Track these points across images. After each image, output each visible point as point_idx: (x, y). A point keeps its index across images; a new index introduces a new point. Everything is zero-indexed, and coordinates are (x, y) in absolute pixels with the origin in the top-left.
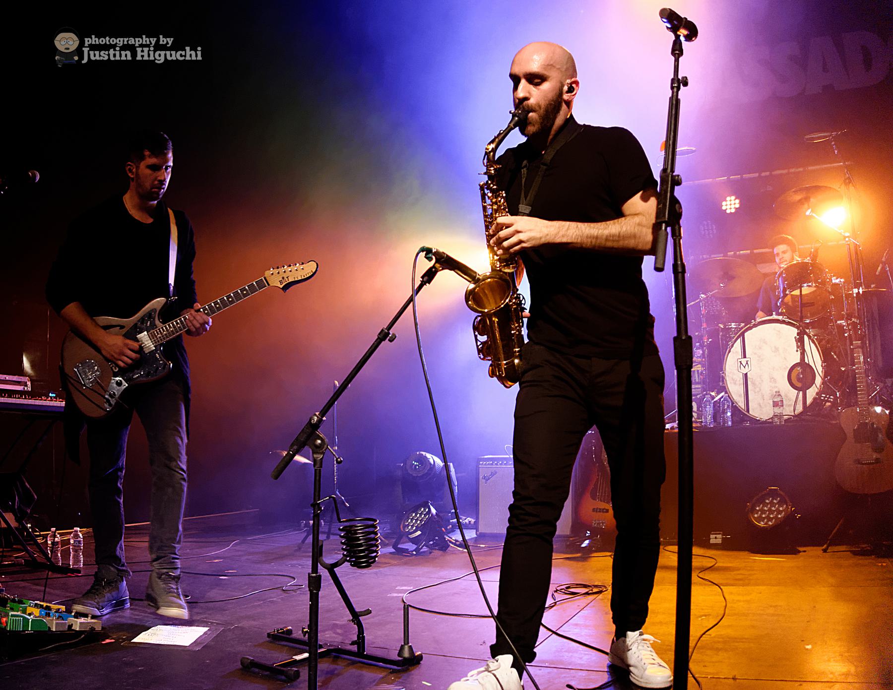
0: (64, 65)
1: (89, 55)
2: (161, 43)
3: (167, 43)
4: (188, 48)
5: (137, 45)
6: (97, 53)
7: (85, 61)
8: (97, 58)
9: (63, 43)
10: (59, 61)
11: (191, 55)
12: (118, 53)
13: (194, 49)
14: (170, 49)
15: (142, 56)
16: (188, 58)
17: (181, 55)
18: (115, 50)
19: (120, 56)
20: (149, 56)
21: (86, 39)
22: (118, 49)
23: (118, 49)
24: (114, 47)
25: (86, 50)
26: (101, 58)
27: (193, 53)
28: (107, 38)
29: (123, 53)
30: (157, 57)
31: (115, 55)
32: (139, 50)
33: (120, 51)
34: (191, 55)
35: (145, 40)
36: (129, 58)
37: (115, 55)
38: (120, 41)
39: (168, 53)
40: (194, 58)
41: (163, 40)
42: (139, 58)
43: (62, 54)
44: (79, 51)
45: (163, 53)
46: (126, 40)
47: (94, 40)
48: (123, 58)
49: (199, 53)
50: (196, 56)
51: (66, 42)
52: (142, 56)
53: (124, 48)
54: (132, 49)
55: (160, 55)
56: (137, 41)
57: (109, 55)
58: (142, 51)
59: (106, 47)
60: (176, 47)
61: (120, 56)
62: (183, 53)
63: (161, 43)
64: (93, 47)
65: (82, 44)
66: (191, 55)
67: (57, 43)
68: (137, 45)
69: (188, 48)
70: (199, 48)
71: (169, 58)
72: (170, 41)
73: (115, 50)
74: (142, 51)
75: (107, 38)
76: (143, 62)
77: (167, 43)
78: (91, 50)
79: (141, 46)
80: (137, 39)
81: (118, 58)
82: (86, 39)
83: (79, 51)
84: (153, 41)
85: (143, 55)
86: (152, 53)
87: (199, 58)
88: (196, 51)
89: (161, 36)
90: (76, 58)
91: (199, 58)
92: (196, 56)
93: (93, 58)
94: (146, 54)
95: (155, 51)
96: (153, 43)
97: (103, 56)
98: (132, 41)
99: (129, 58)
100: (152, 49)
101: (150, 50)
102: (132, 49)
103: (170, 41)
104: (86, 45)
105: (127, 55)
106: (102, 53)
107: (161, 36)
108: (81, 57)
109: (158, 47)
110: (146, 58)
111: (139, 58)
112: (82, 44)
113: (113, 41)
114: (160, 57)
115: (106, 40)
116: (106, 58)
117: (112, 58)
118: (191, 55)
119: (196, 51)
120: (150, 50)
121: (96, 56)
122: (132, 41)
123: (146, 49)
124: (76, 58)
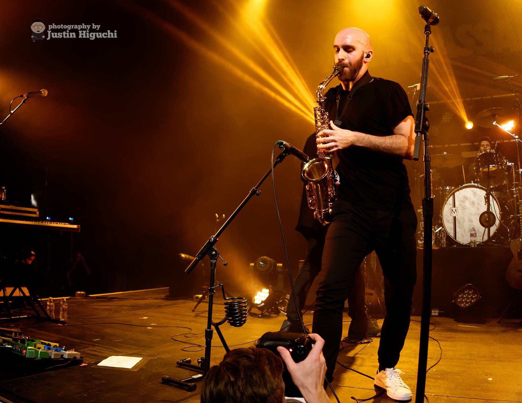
0: (36, 41)
1: (51, 35)
2: (93, 28)
3: (97, 28)
4: (109, 31)
5: (79, 29)
6: (56, 34)
7: (49, 38)
8: (56, 37)
9: (36, 28)
10: (34, 38)
11: (111, 35)
12: (68, 34)
13: (112, 31)
14: (98, 31)
15: (82, 36)
16: (109, 37)
17: (105, 35)
18: (66, 32)
19: (69, 35)
20: (86, 35)
21: (49, 26)
22: (68, 31)
23: (68, 31)
24: (66, 30)
25: (49, 32)
26: (58, 37)
27: (112, 34)
28: (62, 25)
29: (71, 34)
30: (91, 36)
31: (66, 35)
32: (80, 32)
33: (69, 32)
34: (111, 35)
35: (84, 26)
37: (66, 35)
38: (69, 27)
39: (97, 34)
40: (112, 37)
41: (94, 26)
42: (80, 37)
44: (45, 33)
45: (94, 34)
46: (73, 26)
47: (54, 26)
48: (71, 37)
49: (115, 34)
50: (114, 35)
51: (38, 27)
52: (82, 36)
53: (72, 31)
54: (76, 31)
55: (92, 35)
56: (79, 27)
57: (63, 35)
58: (82, 33)
59: (61, 31)
60: (102, 30)
61: (69, 35)
62: (106, 34)
63: (93, 28)
64: (53, 31)
65: (47, 29)
66: (111, 35)
67: (32, 28)
68: (79, 29)
69: (109, 31)
70: (116, 31)
71: (98, 37)
72: (99, 27)
73: (66, 32)
74: (82, 33)
75: (62, 25)
76: (82, 39)
77: (97, 28)
78: (52, 32)
79: (82, 29)
80: (79, 26)
81: (68, 37)
82: (49, 26)
83: (45, 33)
85: (82, 35)
86: (88, 34)
87: (116, 37)
88: (114, 32)
89: (93, 24)
90: (44, 37)
91: (116, 37)
92: (114, 35)
93: (53, 37)
94: (84, 34)
95: (89, 33)
96: (89, 28)
97: (59, 35)
98: (76, 27)
99: (75, 37)
100: (88, 31)
101: (86, 32)
102: (76, 31)
103: (99, 27)
104: (49, 29)
105: (73, 35)
106: (59, 34)
107: (93, 24)
108: (47, 37)
109: (92, 30)
110: (84, 37)
111: (80, 37)
112: (47, 29)
113: (65, 27)
114: (93, 36)
115: (61, 26)
116: (61, 37)
117: (65, 37)
118: (111, 35)
119: (114, 32)
120: (86, 32)
121: (55, 36)
122: (76, 27)
123: (84, 32)
124: (44, 37)
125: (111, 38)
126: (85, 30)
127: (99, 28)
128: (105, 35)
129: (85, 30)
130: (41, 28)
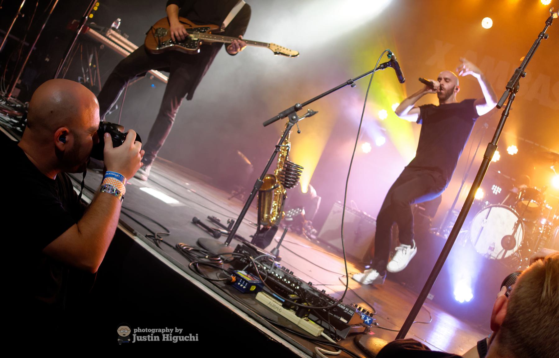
0: (122, 344)
4: (191, 335)
6: (141, 337)
8: (141, 340)
9: (122, 331)
12: (152, 337)
14: (181, 335)
15: (166, 339)
16: (191, 340)
17: (187, 338)
18: (151, 336)
20: (169, 339)
24: (150, 334)
25: (134, 335)
27: (194, 337)
31: (150, 338)
32: (164, 335)
35: (167, 330)
36: (158, 340)
37: (150, 338)
38: (153, 331)
39: (180, 337)
40: (194, 340)
41: (177, 330)
42: (164, 340)
43: (121, 337)
44: (131, 336)
45: (177, 337)
47: (139, 330)
48: (155, 340)
49: (197, 337)
51: (123, 331)
52: (166, 339)
53: (156, 334)
54: (160, 335)
57: (147, 338)
58: (166, 336)
59: (146, 334)
60: (184, 334)
62: (188, 337)
64: (138, 334)
65: (132, 332)
67: (118, 332)
69: (191, 335)
70: (197, 335)
71: (180, 340)
72: (181, 330)
74: (166, 336)
79: (165, 333)
81: (152, 340)
83: (131, 336)
84: (172, 330)
85: (166, 338)
86: (171, 337)
88: (195, 336)
90: (129, 340)
91: (197, 340)
93: (138, 340)
94: (167, 337)
95: (172, 336)
96: (172, 331)
98: (160, 331)
99: (158, 340)
101: (170, 336)
102: (160, 335)
103: (181, 330)
105: (157, 339)
106: (143, 337)
108: (132, 340)
109: (174, 334)
110: (168, 340)
111: (164, 340)
112: (132, 332)
113: (150, 330)
114: (175, 339)
116: (146, 340)
117: (149, 340)
119: (195, 336)
120: (170, 336)
121: (141, 339)
122: (160, 331)
123: (168, 335)
124: (129, 340)
125: (193, 341)
126: (169, 333)
127: (181, 331)
128: (187, 338)
129: (169, 333)
130: (126, 331)
